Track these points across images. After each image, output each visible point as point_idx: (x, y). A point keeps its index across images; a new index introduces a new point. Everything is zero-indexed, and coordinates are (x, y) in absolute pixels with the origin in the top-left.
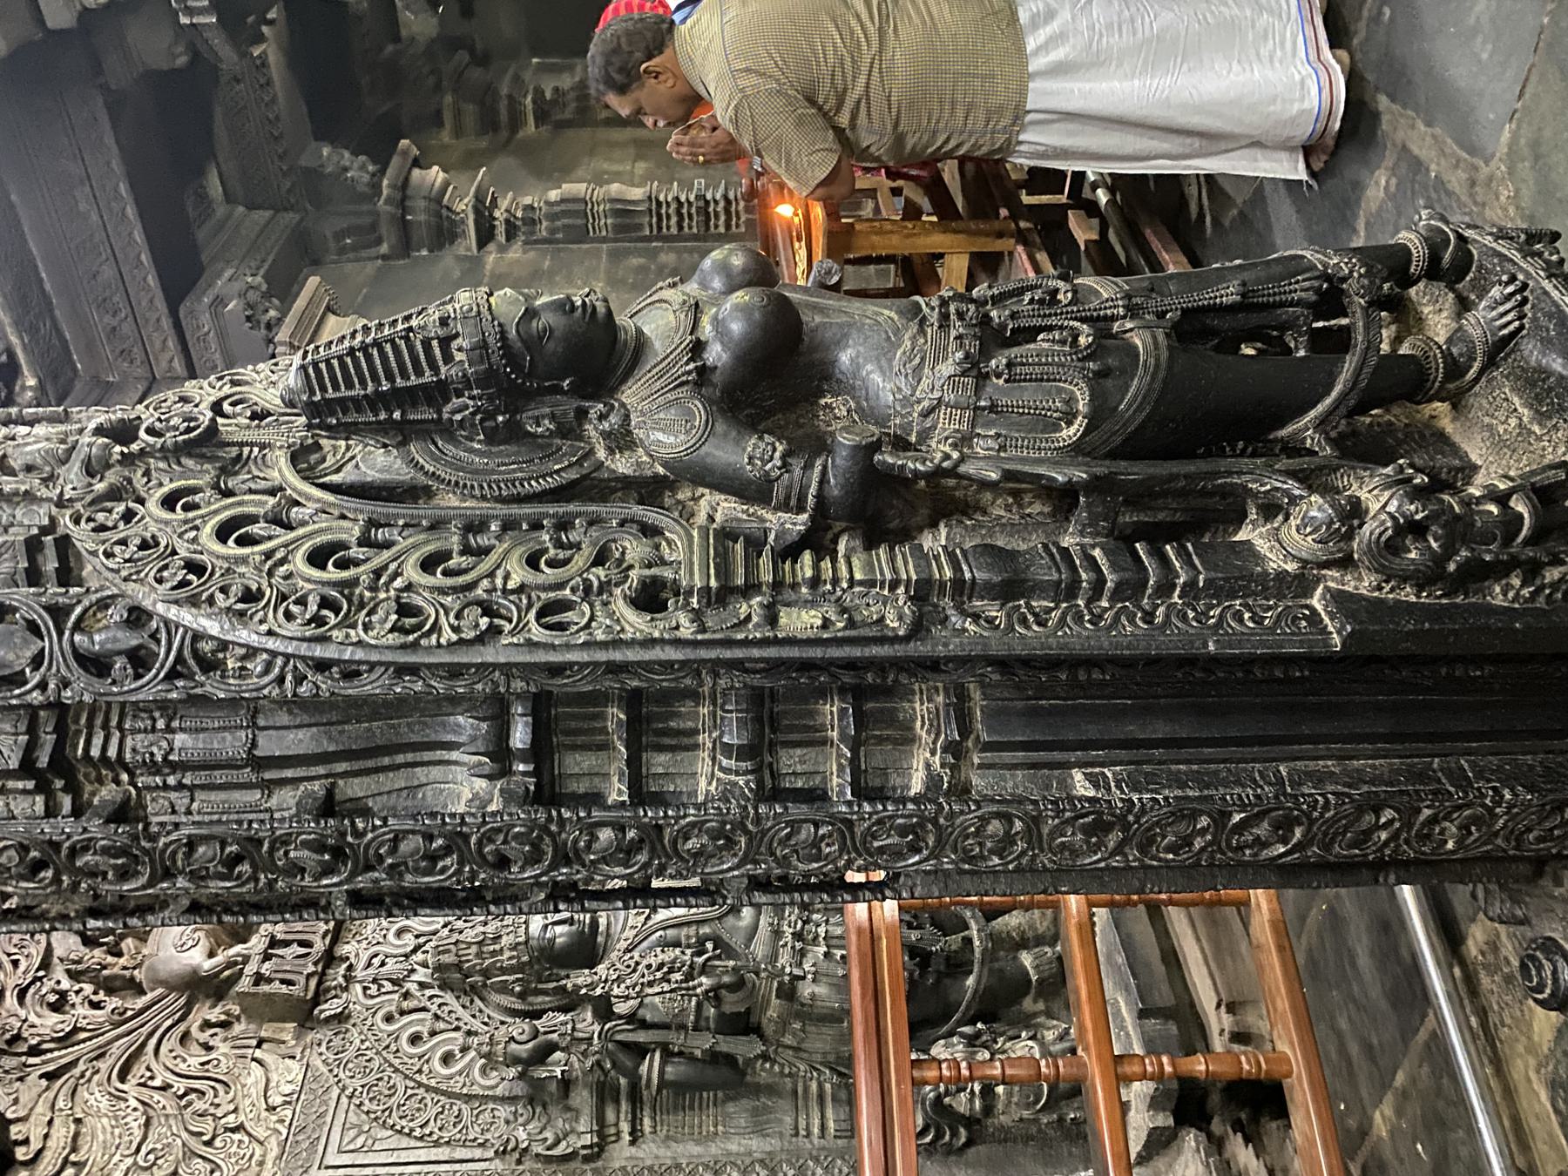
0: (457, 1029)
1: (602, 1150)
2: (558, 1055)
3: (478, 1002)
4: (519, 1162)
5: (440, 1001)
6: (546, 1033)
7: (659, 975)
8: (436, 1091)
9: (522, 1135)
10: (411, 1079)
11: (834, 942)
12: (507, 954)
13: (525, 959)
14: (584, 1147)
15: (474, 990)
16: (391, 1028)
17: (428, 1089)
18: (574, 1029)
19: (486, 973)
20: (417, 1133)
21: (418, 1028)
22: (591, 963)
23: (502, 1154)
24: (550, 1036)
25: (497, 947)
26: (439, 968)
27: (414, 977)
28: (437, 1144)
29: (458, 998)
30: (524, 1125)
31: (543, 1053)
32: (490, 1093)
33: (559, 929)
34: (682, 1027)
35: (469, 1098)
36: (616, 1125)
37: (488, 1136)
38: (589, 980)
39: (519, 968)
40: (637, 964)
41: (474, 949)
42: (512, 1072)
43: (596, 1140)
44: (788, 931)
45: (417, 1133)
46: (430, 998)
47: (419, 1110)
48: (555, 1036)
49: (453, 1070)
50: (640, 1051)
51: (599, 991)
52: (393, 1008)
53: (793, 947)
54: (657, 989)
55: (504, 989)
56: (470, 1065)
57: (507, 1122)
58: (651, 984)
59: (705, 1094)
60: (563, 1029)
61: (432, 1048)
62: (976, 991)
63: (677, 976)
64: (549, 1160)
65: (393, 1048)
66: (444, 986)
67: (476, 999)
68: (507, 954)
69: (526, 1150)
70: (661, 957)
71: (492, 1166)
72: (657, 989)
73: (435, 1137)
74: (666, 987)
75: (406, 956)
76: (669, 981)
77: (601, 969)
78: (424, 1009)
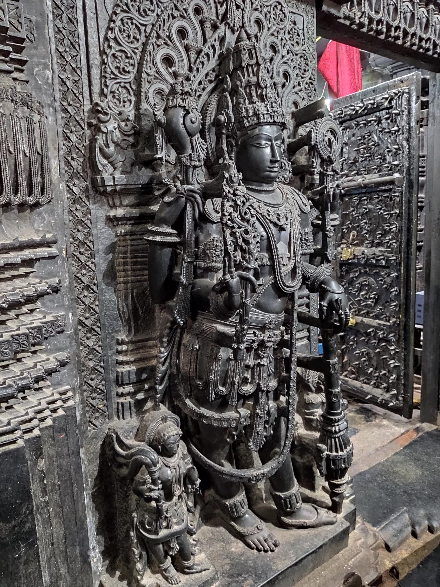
0: (191, 69)
1: (104, 193)
2: (173, 155)
3: (210, 87)
4: (90, 125)
5: (211, 55)
6: (191, 142)
7: (240, 241)
8: (144, 51)
9: (111, 126)
10: (152, 29)
11: (257, 370)
12: (250, 108)
13: (247, 124)
14: (103, 179)
15: (219, 83)
16: (191, 12)
17: (145, 45)
18: (195, 167)
19: (234, 92)
20: (110, 34)
21: (191, 35)
22: (246, 181)
23: (95, 110)
24: (189, 145)
25: (255, 99)
26: (237, 51)
27: (228, 32)
28: (102, 53)
29: (214, 70)
30: (119, 127)
31: (175, 140)
32: (143, 98)
33: (268, 151)
34: (197, 257)
35: (138, 79)
36: (121, 205)
37: (110, 97)
38: (235, 180)
39: (239, 120)
40: (248, 221)
41: (254, 79)
42: (160, 113)
43: (109, 189)
44: (265, 336)
45: (110, 34)
46: (213, 47)
47: (129, 36)
48: (190, 151)
49: (160, 65)
50: (179, 225)
51: (226, 189)
52: (206, 14)
53: (254, 342)
54: (229, 239)
55: (221, 107)
56: (163, 79)
57: (120, 114)
58: (233, 234)
59: (146, 272)
60: (195, 158)
61: (176, 47)
62: (222, 473)
63: (239, 258)
64: (91, 149)
65: (176, 13)
66: (223, 58)
67: (213, 85)
68: (250, 108)
69: (100, 130)
70: (253, 241)
71: (87, 102)
72: (229, 239)
73: (108, 51)
74: (231, 248)
75: (243, 26)
76: (235, 250)
77: (242, 190)
78: (205, 41)
